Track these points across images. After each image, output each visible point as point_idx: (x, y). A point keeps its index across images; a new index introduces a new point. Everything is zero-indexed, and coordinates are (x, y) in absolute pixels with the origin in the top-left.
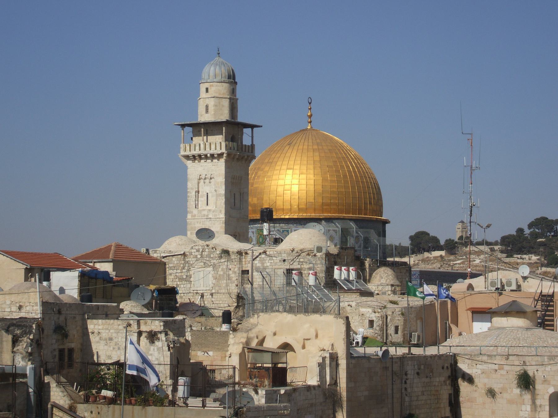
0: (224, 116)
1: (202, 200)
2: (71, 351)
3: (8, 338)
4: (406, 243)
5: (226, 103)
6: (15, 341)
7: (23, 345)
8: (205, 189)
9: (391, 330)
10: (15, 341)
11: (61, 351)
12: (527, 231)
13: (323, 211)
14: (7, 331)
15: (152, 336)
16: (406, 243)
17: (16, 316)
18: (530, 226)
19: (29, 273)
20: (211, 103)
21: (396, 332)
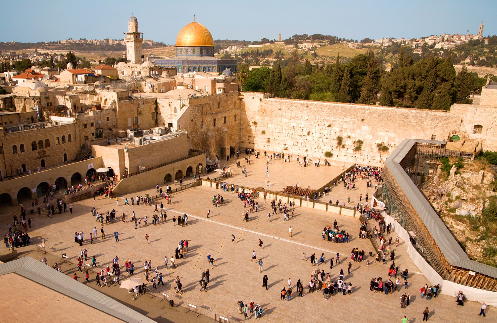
0: (134, 31)
1: (130, 52)
2: (51, 103)
3: (33, 101)
4: (261, 41)
5: (134, 28)
6: (35, 102)
7: (36, 103)
8: (130, 49)
9: (155, 89)
10: (35, 102)
11: (48, 104)
12: (292, 38)
13: (196, 44)
14: (33, 99)
15: (67, 99)
16: (261, 41)
17: (35, 96)
18: (293, 37)
19: (73, 75)
20: (131, 28)
21: (156, 89)
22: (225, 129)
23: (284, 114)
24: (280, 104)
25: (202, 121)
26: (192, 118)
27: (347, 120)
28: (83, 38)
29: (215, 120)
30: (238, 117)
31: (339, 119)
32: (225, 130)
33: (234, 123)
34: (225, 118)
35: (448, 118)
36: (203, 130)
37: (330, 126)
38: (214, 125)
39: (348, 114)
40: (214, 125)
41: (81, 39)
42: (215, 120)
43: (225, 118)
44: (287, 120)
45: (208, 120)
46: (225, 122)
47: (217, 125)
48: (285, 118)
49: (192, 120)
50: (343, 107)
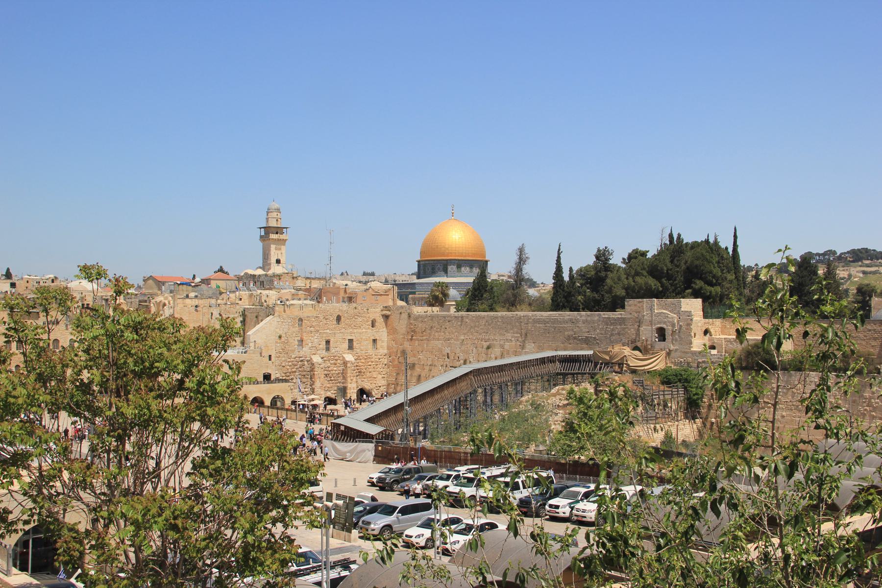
22: (349, 357)
23: (437, 334)
24: (432, 320)
25: (301, 341)
26: (280, 333)
27: (509, 336)
28: (370, 271)
29: (328, 342)
30: (379, 343)
31: (501, 334)
32: (347, 359)
33: (371, 351)
34: (351, 341)
35: (622, 321)
36: (302, 354)
37: (488, 348)
38: (328, 349)
39: (509, 327)
40: (328, 349)
41: (365, 274)
42: (328, 342)
43: (351, 341)
44: (438, 344)
45: (314, 340)
46: (351, 347)
47: (333, 350)
48: (438, 339)
49: (280, 337)
50: (502, 317)
